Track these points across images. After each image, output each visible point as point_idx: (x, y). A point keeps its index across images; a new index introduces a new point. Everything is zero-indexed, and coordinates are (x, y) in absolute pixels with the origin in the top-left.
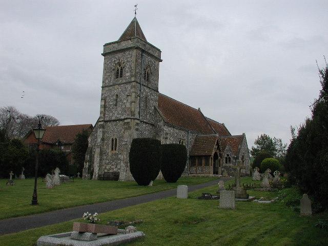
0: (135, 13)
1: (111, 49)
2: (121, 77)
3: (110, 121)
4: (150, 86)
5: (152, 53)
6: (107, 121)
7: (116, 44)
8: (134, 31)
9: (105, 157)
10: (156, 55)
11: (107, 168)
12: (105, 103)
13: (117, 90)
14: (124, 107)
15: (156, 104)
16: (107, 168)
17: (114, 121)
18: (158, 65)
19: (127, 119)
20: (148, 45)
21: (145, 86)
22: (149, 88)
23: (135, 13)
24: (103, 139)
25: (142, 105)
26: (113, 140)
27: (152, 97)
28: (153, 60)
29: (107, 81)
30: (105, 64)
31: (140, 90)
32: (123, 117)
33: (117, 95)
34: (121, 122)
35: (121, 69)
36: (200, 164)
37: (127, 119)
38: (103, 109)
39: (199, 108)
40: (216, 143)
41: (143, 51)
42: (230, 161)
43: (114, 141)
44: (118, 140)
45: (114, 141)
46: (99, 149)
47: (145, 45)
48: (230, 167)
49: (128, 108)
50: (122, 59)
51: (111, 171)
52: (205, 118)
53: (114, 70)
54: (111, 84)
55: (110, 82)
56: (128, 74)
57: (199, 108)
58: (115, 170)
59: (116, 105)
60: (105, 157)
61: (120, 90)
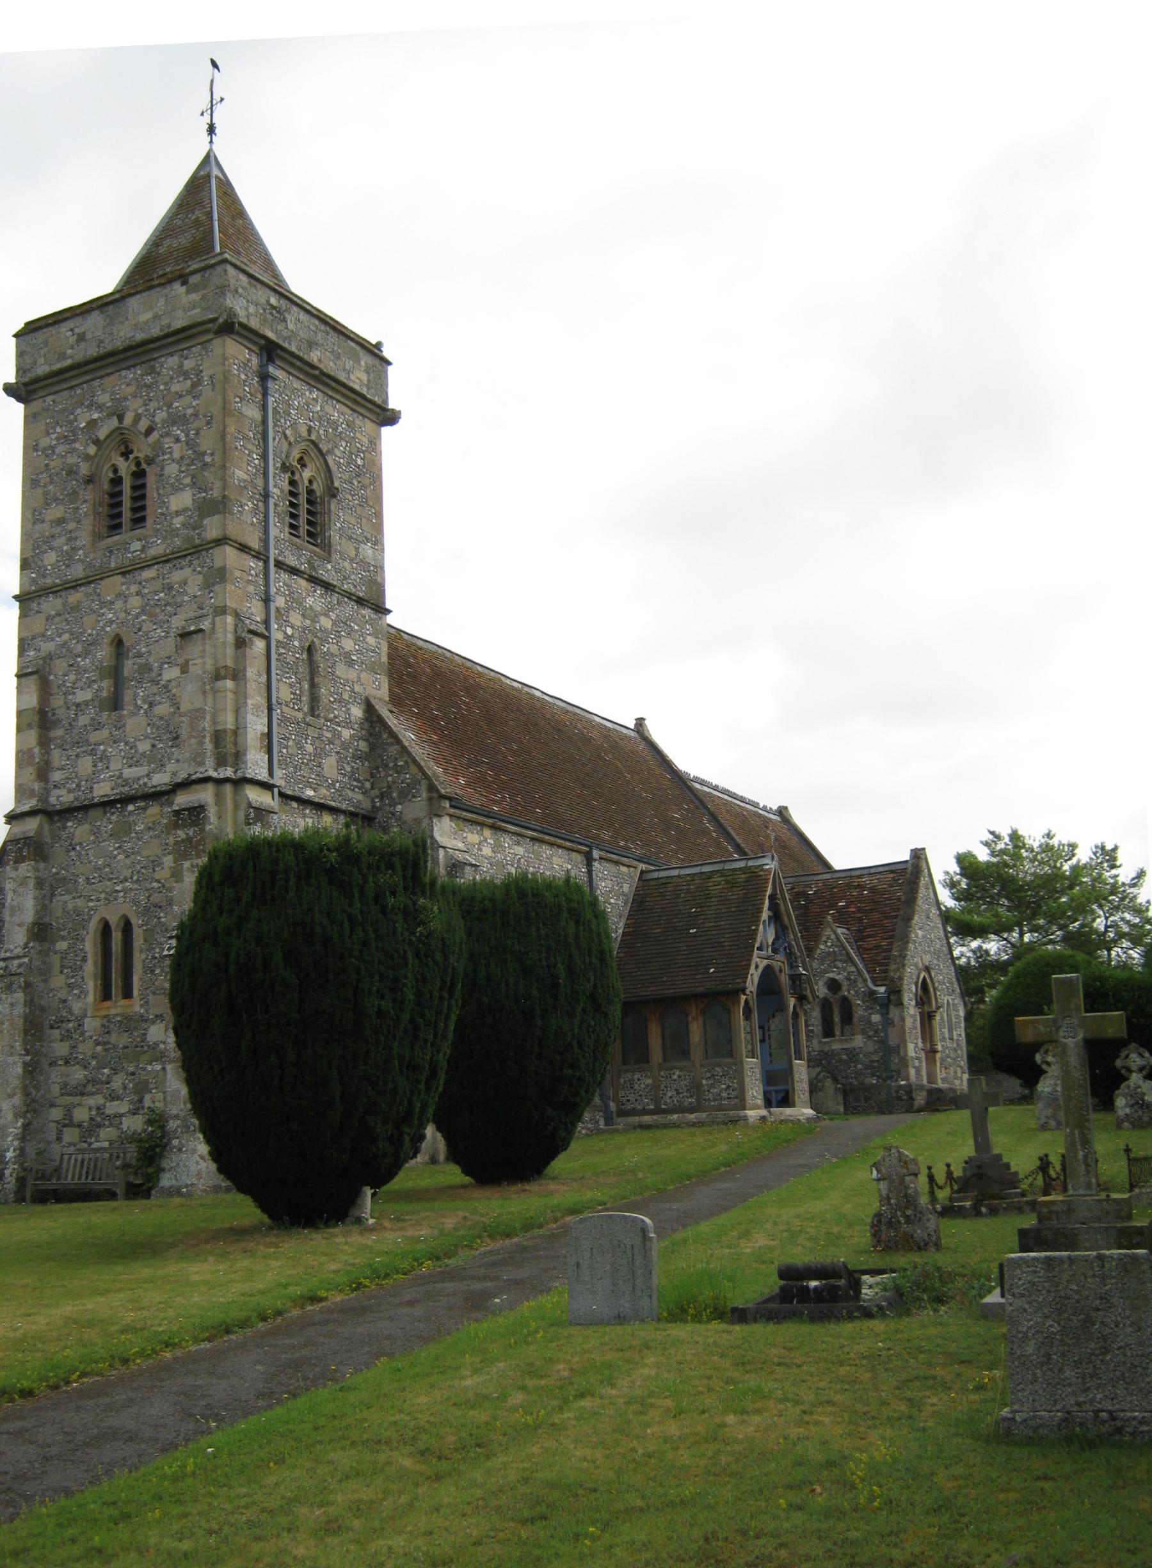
0: (211, 130)
1: (69, 347)
2: (139, 521)
4: (326, 571)
5: (329, 366)
6: (68, 812)
7: (95, 319)
9: (61, 1049)
10: (358, 379)
11: (81, 1115)
13: (120, 605)
14: (163, 709)
15: (379, 689)
16: (81, 1115)
17: (107, 805)
18: (374, 444)
19: (186, 784)
20: (303, 316)
21: (294, 571)
22: (327, 587)
23: (211, 130)
24: (41, 932)
25: (283, 692)
26: (106, 930)
27: (348, 644)
28: (337, 412)
29: (51, 557)
30: (31, 447)
31: (267, 600)
32: (161, 779)
33: (118, 642)
34: (154, 810)
35: (139, 474)
36: (678, 1049)
37: (186, 784)
38: (32, 736)
39: (640, 722)
40: (765, 914)
41: (270, 351)
42: (847, 1017)
43: (117, 937)
44: (138, 941)
45: (117, 937)
46: (19, 996)
47: (279, 315)
48: (853, 1054)
49: (197, 715)
50: (134, 406)
51: (105, 1137)
52: (680, 779)
53: (90, 480)
54: (78, 571)
55: (68, 559)
56: (183, 500)
57: (640, 722)
59: (115, 703)
61: (135, 602)
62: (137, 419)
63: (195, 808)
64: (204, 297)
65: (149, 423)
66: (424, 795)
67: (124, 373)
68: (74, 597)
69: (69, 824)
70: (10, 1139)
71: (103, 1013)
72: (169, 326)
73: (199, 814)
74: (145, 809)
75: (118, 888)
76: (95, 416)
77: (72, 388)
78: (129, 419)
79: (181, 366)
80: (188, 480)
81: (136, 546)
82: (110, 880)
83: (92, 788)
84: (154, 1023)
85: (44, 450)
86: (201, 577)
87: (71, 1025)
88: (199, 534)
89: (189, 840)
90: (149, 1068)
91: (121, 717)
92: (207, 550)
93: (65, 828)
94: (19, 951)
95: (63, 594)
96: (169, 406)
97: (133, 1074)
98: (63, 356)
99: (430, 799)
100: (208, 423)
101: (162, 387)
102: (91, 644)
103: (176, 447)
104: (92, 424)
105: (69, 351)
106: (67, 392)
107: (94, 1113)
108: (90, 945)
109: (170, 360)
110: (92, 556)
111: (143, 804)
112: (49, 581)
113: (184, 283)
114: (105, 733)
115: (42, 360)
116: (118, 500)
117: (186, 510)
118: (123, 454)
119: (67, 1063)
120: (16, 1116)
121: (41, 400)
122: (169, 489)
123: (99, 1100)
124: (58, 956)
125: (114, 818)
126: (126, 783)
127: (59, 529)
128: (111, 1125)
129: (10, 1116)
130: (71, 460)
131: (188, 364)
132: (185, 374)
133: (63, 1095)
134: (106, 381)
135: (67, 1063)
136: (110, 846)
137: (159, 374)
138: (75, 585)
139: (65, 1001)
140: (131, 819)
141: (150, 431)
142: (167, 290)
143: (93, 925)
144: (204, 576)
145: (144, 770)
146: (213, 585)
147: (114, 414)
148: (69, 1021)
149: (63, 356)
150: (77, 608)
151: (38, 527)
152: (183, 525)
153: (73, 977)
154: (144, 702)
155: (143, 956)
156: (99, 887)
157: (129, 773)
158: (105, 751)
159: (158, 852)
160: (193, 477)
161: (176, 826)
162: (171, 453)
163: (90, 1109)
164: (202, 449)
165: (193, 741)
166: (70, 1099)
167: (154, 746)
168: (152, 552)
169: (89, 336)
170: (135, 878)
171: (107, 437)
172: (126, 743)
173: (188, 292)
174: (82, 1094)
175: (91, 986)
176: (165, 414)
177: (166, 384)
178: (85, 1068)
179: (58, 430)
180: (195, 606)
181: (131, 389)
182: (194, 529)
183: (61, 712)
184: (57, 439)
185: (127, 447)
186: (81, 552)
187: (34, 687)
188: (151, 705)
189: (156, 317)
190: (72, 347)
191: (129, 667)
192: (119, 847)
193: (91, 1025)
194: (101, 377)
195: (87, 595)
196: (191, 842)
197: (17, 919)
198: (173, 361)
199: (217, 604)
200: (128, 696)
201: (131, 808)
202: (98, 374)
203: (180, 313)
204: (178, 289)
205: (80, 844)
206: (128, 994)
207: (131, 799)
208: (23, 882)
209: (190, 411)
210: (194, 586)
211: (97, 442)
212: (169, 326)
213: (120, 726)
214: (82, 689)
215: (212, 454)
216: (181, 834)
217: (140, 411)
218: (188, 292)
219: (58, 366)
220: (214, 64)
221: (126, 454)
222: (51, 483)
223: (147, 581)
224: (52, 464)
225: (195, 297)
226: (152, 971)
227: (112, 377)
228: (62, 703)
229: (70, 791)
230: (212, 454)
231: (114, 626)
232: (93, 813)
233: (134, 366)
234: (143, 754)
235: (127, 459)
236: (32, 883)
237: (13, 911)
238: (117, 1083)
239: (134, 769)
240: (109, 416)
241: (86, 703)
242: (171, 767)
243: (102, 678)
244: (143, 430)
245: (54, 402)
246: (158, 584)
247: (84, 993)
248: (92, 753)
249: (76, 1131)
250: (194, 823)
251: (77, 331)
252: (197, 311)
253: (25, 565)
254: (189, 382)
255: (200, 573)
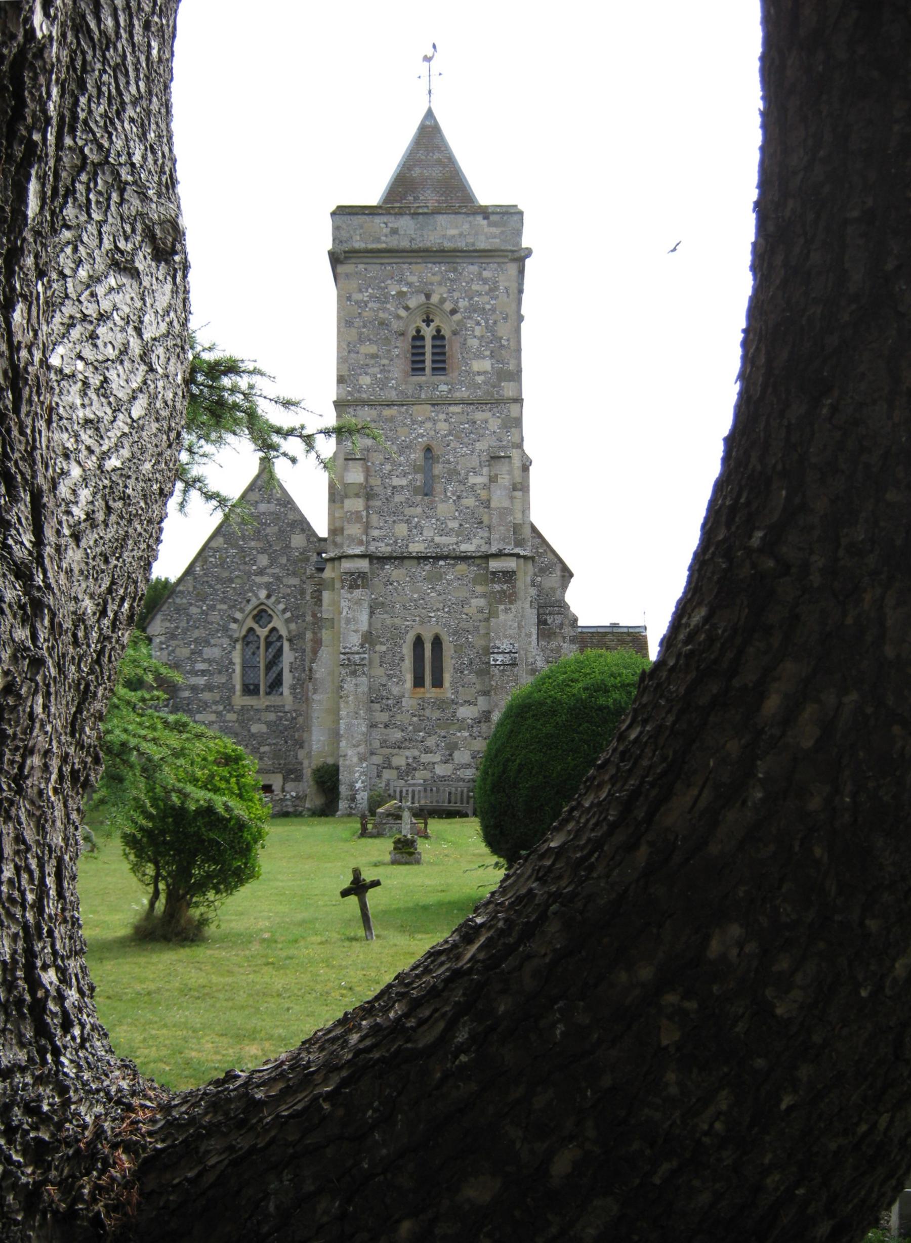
0: (430, 92)
3: (400, 559)
8: (428, 176)
9: (384, 717)
12: (367, 472)
14: (470, 502)
16: (399, 761)
17: (421, 559)
19: (499, 555)
24: (369, 639)
26: (419, 642)
29: (365, 380)
33: (428, 450)
34: (462, 567)
35: (438, 336)
37: (499, 555)
43: (428, 647)
45: (428, 647)
49: (505, 512)
51: (420, 776)
54: (393, 395)
55: (383, 384)
56: (486, 365)
58: (440, 770)
59: (427, 491)
60: (384, 717)
61: (443, 427)
62: (443, 301)
63: (508, 572)
64: (502, 233)
65: (452, 306)
66: (559, 573)
67: (430, 265)
68: (387, 412)
69: (387, 567)
70: (357, 775)
71: (420, 696)
72: (473, 244)
73: (511, 576)
74: (454, 565)
75: (432, 615)
76: (405, 289)
77: (382, 264)
78: (435, 299)
79: (480, 274)
80: (488, 353)
81: (444, 388)
82: (423, 608)
83: (407, 545)
84: (462, 705)
85: (357, 302)
86: (500, 420)
87: (390, 702)
88: (498, 392)
89: (504, 592)
90: (459, 734)
91: (433, 502)
92: (505, 404)
93: (383, 569)
94: (356, 649)
95: (378, 408)
96: (471, 299)
97: (445, 737)
98: (378, 240)
99: (563, 576)
100: (504, 318)
101: (464, 284)
102: (407, 447)
103: (477, 329)
104: (401, 294)
105: (383, 238)
106: (378, 267)
107: (410, 760)
108: (407, 650)
109: (471, 267)
110: (404, 387)
111: (452, 562)
112: (364, 396)
113: (486, 218)
114: (419, 510)
115: (358, 238)
116: (421, 351)
117: (485, 373)
118: (424, 321)
119: (386, 726)
120: (362, 759)
121: (354, 265)
122: (472, 356)
123: (416, 753)
124: (377, 655)
125: (427, 568)
126: (438, 545)
127: (373, 362)
128: (425, 769)
129: (355, 760)
130: (381, 315)
131: (486, 274)
132: (485, 281)
133: (382, 747)
134: (413, 267)
135: (386, 726)
136: (425, 586)
137: (460, 274)
138: (390, 404)
139: (385, 685)
140: (442, 570)
141: (454, 312)
142: (471, 218)
143: (410, 637)
144: (502, 420)
145: (453, 540)
146: (510, 428)
147: (422, 292)
148: (388, 699)
149: (378, 240)
150: (391, 419)
151: (353, 355)
152: (484, 382)
153: (391, 670)
154: (453, 494)
155: (453, 662)
156: (416, 612)
157: (438, 539)
158: (419, 522)
159: (468, 595)
160: (492, 352)
161: (493, 581)
162: (473, 331)
163: (407, 758)
164: (500, 334)
165: (501, 528)
166: (389, 750)
167: (461, 525)
168: (458, 395)
169: (401, 232)
170: (446, 610)
171: (418, 307)
172: (437, 520)
173: (489, 225)
174: (399, 748)
175: (409, 678)
176: (466, 303)
177: (467, 283)
178: (403, 731)
179: (370, 290)
180: (495, 438)
181: (437, 278)
182: (494, 387)
183: (379, 490)
184: (370, 297)
185: (428, 317)
186: (393, 382)
187: (361, 469)
188: (459, 497)
189: (461, 235)
190: (386, 236)
191: (438, 469)
192: (432, 588)
193: (408, 703)
194: (410, 264)
195: (400, 412)
196: (505, 593)
197: (353, 628)
198: (474, 269)
199: (513, 440)
200: (438, 488)
201: (441, 563)
202: (409, 260)
203: (482, 238)
204: (479, 218)
205: (397, 582)
206: (438, 682)
207: (445, 558)
208: (358, 602)
209: (488, 307)
210: (494, 424)
211: (407, 308)
212: (473, 244)
213: (432, 506)
214: (397, 476)
215: (508, 340)
216: (497, 587)
217: (445, 296)
218: (489, 225)
219: (371, 246)
220: (434, 46)
221: (428, 321)
222: (364, 327)
223: (453, 414)
224: (365, 314)
225: (494, 230)
226: (462, 672)
227: (419, 266)
228: (379, 483)
229: (387, 545)
230: (508, 340)
231: (425, 439)
232: (406, 562)
233: (440, 263)
234: (452, 529)
235: (428, 326)
236: (366, 605)
237: (348, 621)
238: (431, 742)
239: (444, 538)
240: (418, 292)
241: (402, 487)
242: (476, 541)
243: (416, 472)
244: (448, 310)
245: (366, 269)
246: (464, 418)
247: (401, 681)
248: (408, 522)
249: (395, 772)
250: (506, 582)
251: (390, 225)
252: (498, 240)
253: (341, 380)
254: (487, 287)
255: (498, 417)
